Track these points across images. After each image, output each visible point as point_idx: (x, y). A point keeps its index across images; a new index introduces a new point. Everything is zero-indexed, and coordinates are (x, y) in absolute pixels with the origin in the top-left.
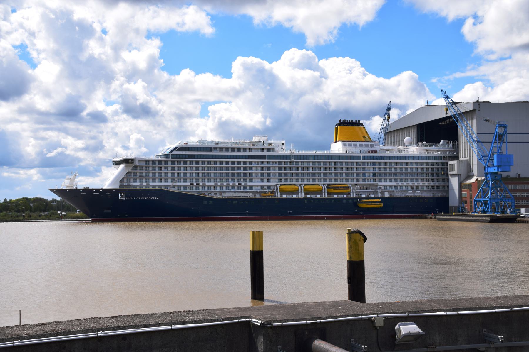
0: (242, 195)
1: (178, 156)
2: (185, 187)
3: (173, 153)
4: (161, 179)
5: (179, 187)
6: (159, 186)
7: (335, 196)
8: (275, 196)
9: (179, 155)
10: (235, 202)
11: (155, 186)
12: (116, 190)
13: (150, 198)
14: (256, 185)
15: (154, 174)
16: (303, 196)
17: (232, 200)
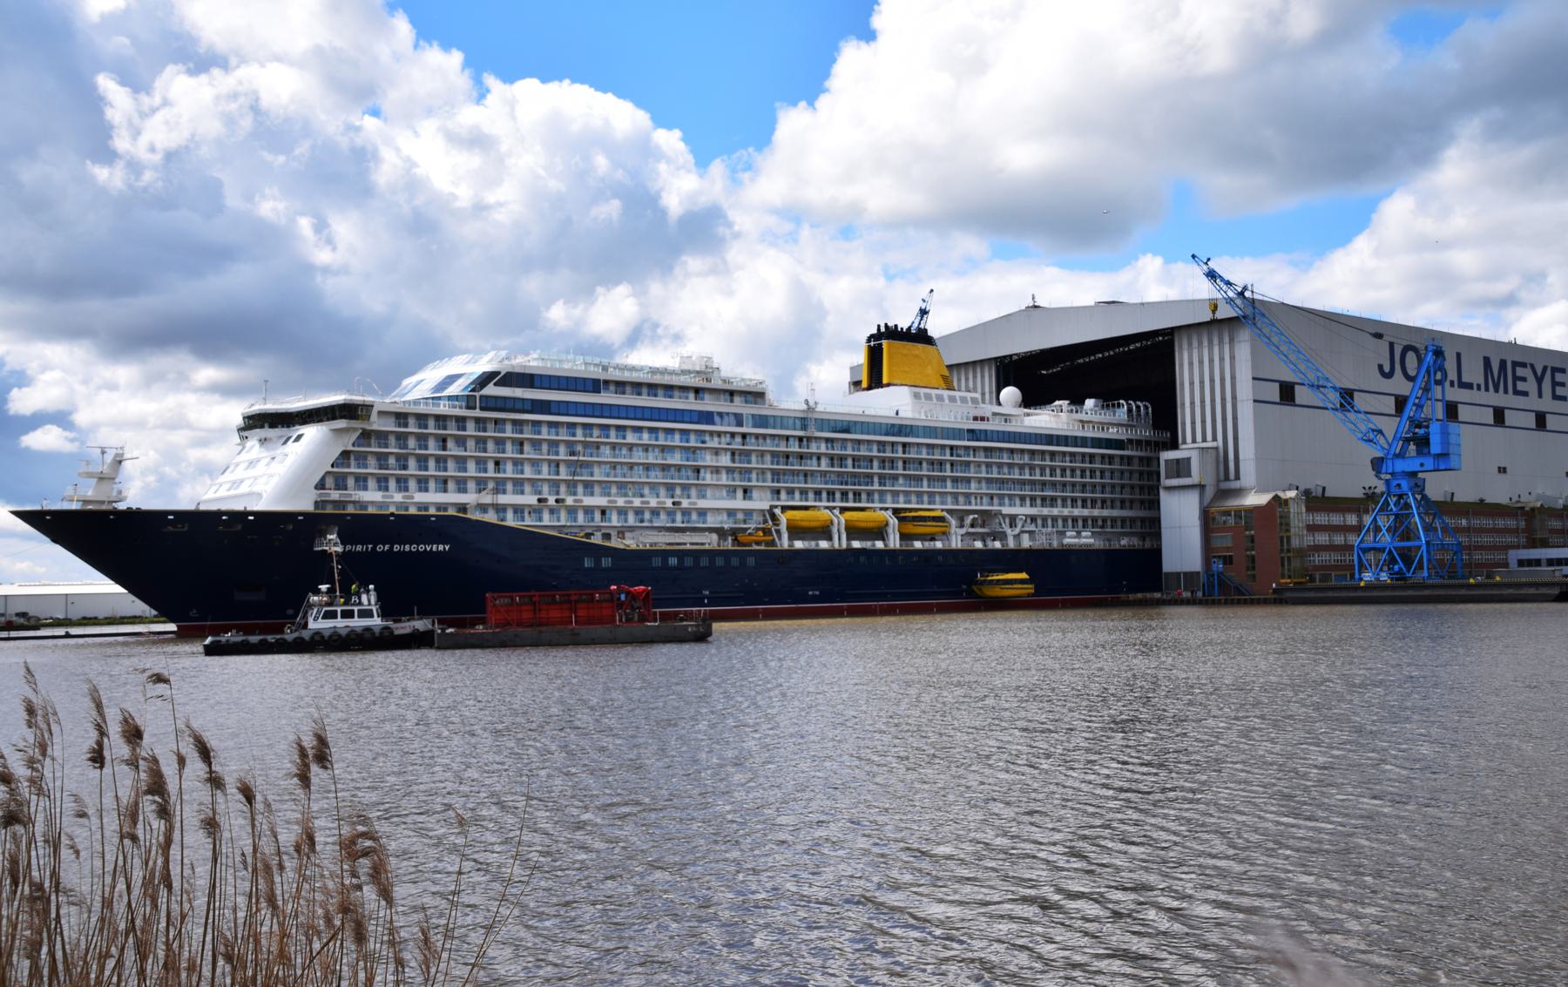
0: (688, 541)
2: (518, 510)
4: (445, 482)
5: (500, 509)
6: (440, 507)
7: (918, 545)
8: (773, 543)
9: (505, 398)
10: (673, 561)
11: (425, 507)
12: (306, 514)
13: (422, 548)
14: (719, 506)
15: (422, 461)
16: (844, 546)
17: (665, 554)
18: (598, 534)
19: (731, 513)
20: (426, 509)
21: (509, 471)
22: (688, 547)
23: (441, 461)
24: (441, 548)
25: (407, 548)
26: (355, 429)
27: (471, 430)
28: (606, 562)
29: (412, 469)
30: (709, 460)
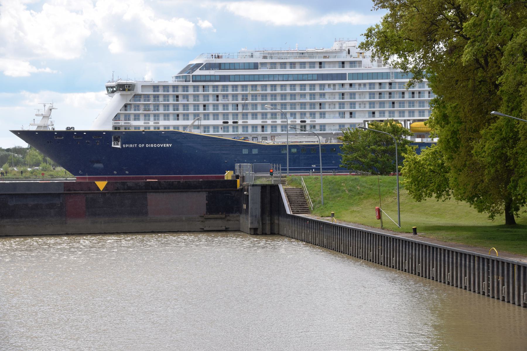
1: (203, 79)
2: (216, 127)
3: (195, 73)
4: (178, 115)
5: (206, 128)
6: (175, 127)
12: (108, 132)
13: (159, 145)
15: (166, 107)
18: (250, 138)
19: (341, 126)
20: (178, 128)
21: (211, 110)
22: (304, 143)
23: (216, 106)
24: (168, 145)
25: (152, 146)
26: (131, 94)
27: (191, 91)
28: (255, 151)
29: (161, 111)
30: (327, 99)
